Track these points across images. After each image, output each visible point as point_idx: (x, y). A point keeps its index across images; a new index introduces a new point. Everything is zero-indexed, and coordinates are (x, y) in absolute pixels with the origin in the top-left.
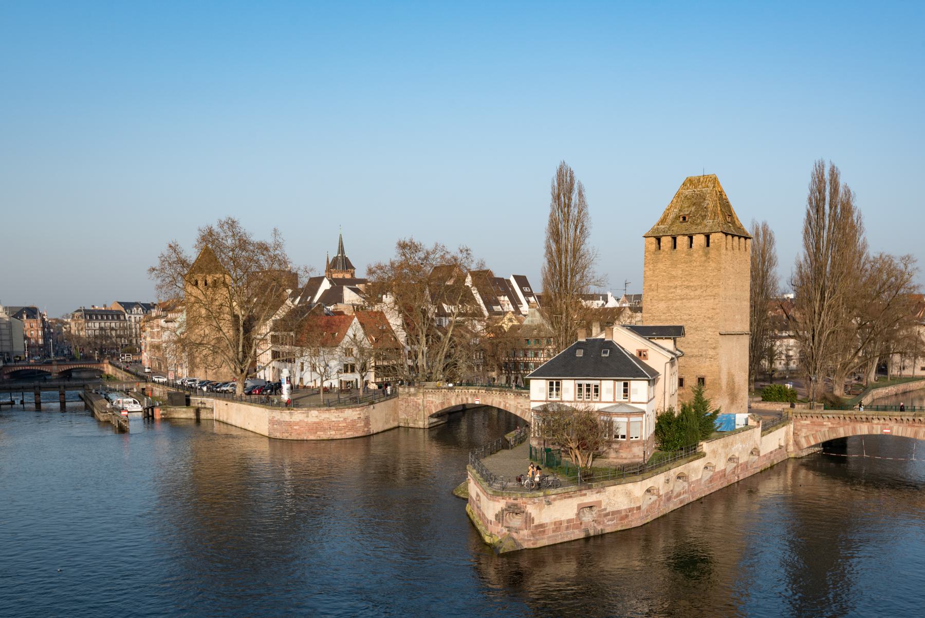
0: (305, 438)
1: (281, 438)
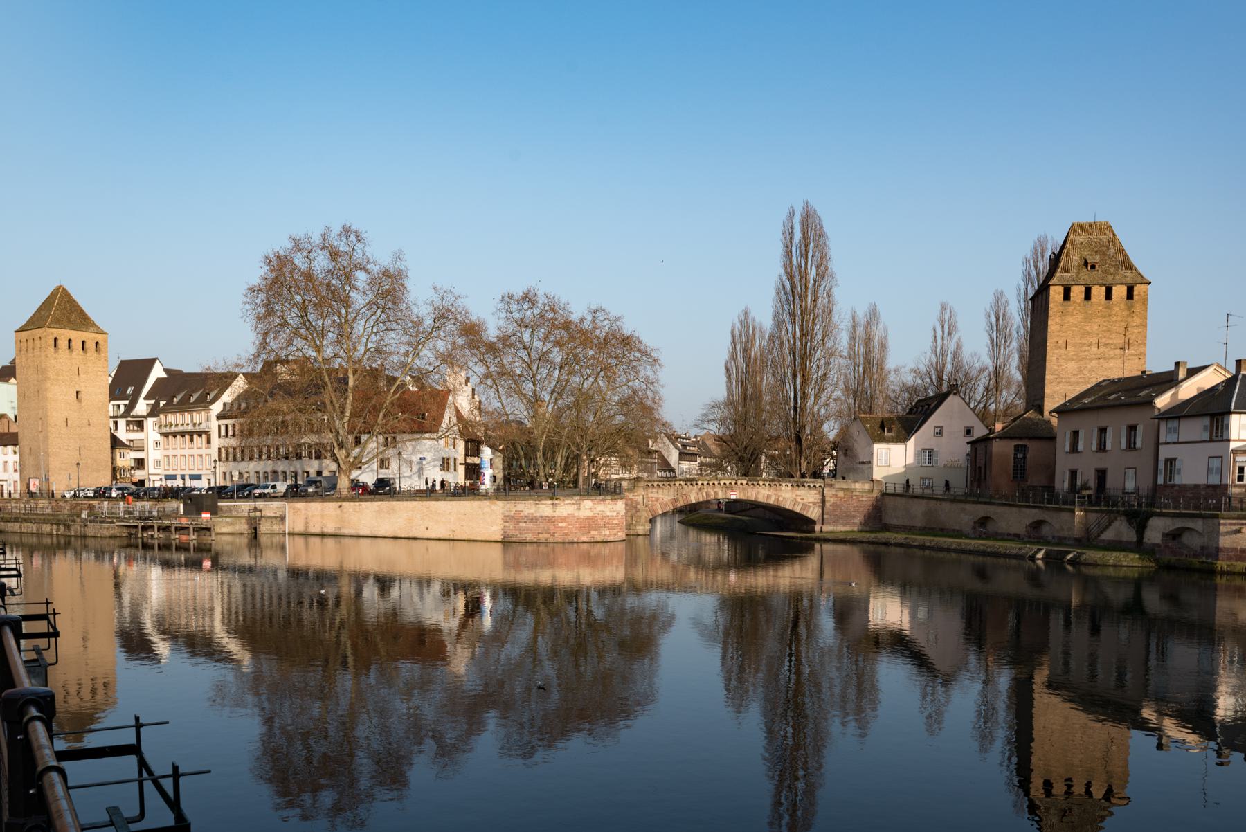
0: (575, 540)
1: (535, 540)
